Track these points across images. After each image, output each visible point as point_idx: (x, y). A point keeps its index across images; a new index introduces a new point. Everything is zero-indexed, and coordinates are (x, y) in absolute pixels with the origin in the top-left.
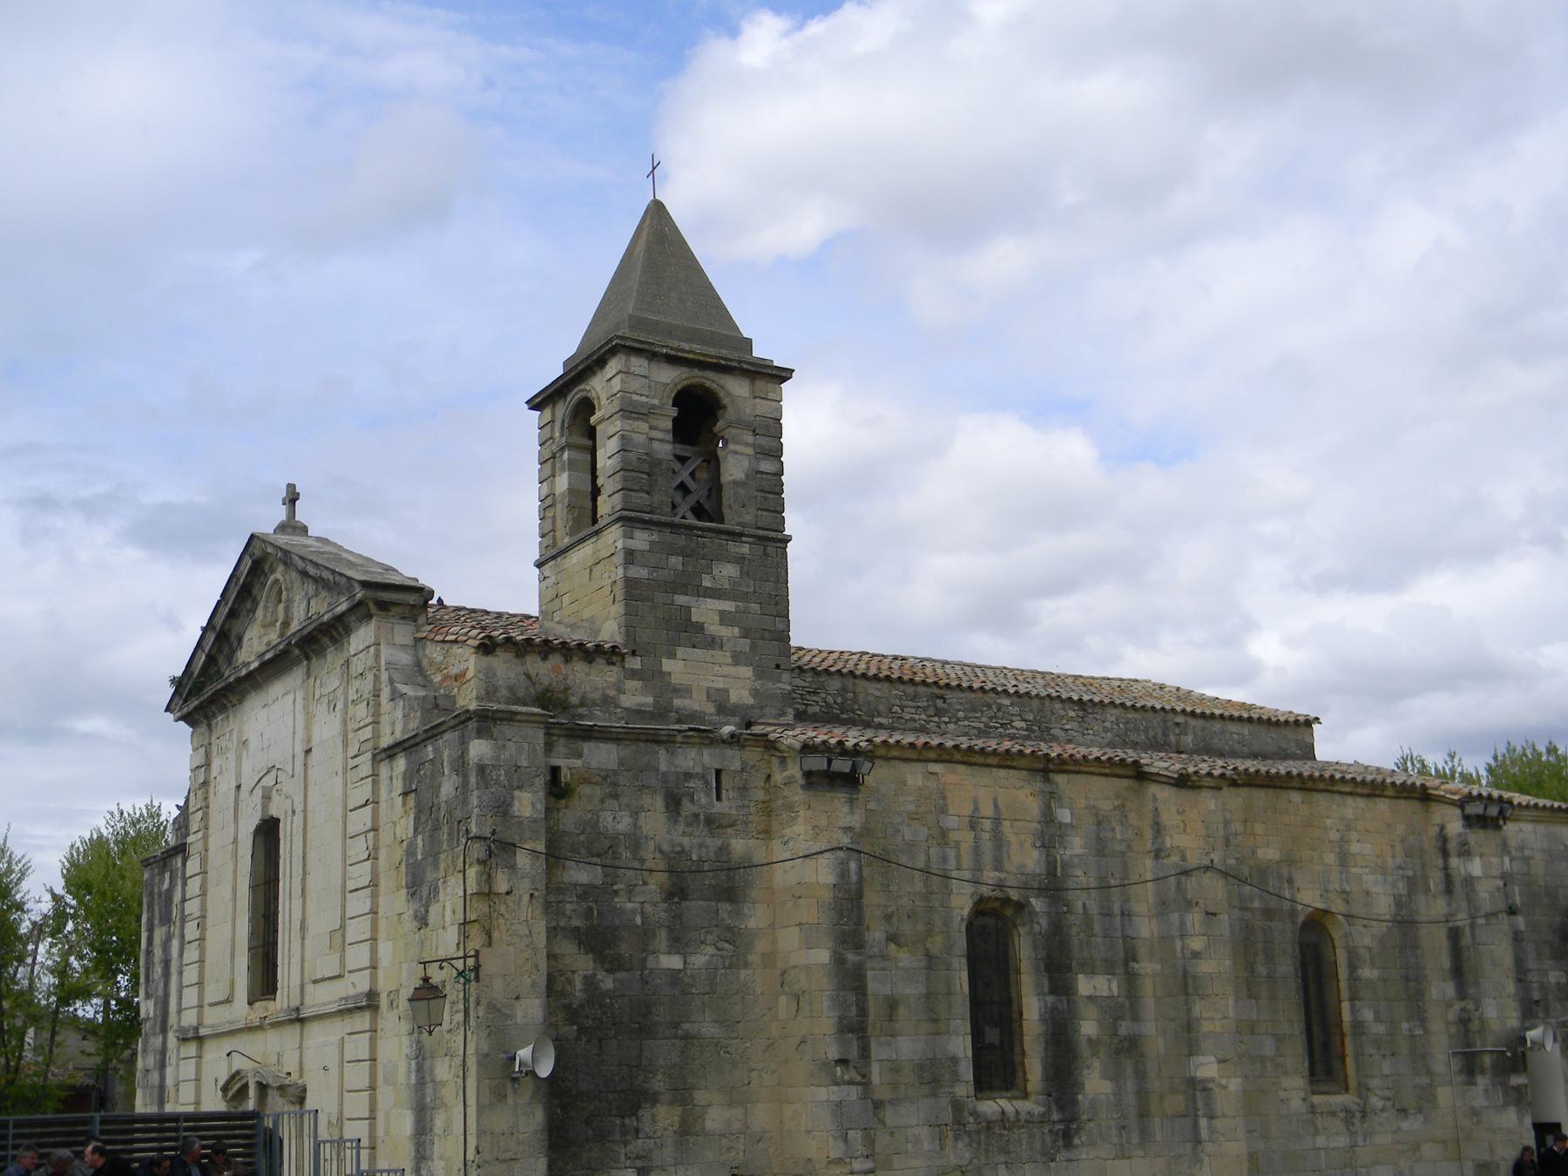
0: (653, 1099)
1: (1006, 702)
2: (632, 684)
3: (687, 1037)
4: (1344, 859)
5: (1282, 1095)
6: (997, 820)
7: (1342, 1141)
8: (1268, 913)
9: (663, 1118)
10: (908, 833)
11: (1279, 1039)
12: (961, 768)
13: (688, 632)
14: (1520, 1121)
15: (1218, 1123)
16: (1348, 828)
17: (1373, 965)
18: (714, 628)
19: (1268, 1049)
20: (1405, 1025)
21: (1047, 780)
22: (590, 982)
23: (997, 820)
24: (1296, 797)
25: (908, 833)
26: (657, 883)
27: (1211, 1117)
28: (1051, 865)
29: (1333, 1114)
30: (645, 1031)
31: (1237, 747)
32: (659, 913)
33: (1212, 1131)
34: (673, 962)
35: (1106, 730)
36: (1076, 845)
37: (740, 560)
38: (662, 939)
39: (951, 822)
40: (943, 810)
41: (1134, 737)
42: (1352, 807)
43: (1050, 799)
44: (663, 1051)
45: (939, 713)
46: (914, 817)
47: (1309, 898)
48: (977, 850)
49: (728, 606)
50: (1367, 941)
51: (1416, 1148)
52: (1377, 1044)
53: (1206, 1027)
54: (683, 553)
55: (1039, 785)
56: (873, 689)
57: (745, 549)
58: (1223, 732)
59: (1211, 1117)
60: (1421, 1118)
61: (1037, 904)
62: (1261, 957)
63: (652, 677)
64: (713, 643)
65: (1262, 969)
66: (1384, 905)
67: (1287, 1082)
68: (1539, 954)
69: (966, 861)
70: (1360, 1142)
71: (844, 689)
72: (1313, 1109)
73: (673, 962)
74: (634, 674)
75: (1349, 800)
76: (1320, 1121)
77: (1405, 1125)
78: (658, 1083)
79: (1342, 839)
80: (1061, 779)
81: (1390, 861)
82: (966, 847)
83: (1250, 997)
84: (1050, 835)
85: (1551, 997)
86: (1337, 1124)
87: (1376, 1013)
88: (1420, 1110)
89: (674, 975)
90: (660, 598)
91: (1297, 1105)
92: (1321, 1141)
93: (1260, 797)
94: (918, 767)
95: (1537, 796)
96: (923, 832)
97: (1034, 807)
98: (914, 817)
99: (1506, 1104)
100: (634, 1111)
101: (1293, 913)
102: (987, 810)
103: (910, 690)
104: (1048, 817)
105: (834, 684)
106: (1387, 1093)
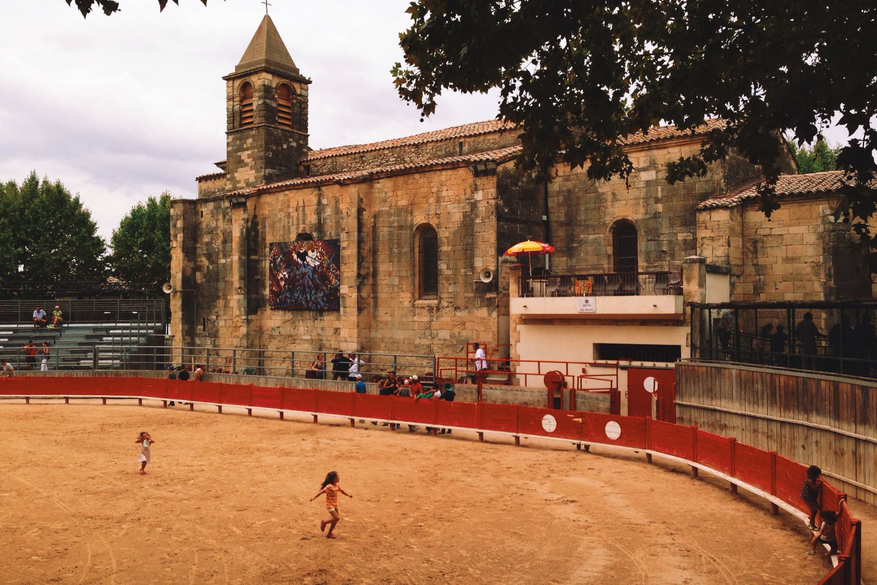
0: (219, 298)
1: (386, 152)
2: (228, 183)
3: (226, 281)
4: (438, 200)
5: (401, 300)
6: (304, 207)
7: (426, 319)
8: (400, 228)
9: (221, 302)
10: (279, 216)
11: (401, 278)
12: (294, 191)
13: (241, 163)
14: (490, 314)
15: (347, 309)
16: (442, 185)
17: (448, 245)
18: (247, 160)
19: (396, 281)
20: (462, 271)
21: (319, 190)
22: (208, 267)
23: (304, 207)
24: (417, 176)
25: (279, 216)
26: (221, 239)
27: (345, 307)
28: (319, 220)
29: (424, 308)
30: (218, 280)
31: (492, 146)
32: (221, 247)
33: (345, 312)
34: (223, 261)
35: (427, 153)
36: (329, 211)
37: (253, 136)
38: (221, 256)
39: (291, 210)
40: (289, 206)
41: (439, 153)
42: (445, 175)
43: (320, 196)
44: (221, 285)
45: (363, 162)
46: (281, 210)
47: (419, 219)
48: (298, 219)
49: (250, 152)
50: (447, 234)
51: (464, 324)
52: (447, 279)
53: (345, 275)
54: (240, 139)
55: (316, 192)
56: (342, 159)
57: (254, 132)
58: (484, 141)
59: (345, 307)
60: (467, 311)
61: (315, 234)
62: (395, 246)
63: (233, 180)
64: (246, 165)
65: (396, 251)
66: (457, 217)
67: (402, 295)
68: (672, 225)
69: (295, 223)
70: (435, 319)
71: (332, 162)
72: (413, 306)
73: (223, 261)
74: (228, 180)
75: (444, 173)
76: (417, 311)
77: (458, 314)
78: (220, 294)
79: (438, 191)
80: (324, 189)
81: (463, 196)
82: (295, 218)
83: (390, 261)
84: (320, 209)
85: (677, 248)
86: (425, 312)
87: (448, 265)
88: (467, 308)
89: (224, 265)
90: (234, 155)
91: (407, 304)
92: (416, 318)
93: (400, 180)
94: (282, 193)
95: (280, 181)
96: (283, 214)
97: (315, 200)
98: (281, 210)
99: (481, 306)
100: (215, 301)
101: (412, 226)
102: (301, 204)
103: (353, 156)
104: (319, 203)
105: (330, 161)
106: (451, 300)
